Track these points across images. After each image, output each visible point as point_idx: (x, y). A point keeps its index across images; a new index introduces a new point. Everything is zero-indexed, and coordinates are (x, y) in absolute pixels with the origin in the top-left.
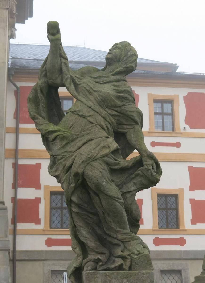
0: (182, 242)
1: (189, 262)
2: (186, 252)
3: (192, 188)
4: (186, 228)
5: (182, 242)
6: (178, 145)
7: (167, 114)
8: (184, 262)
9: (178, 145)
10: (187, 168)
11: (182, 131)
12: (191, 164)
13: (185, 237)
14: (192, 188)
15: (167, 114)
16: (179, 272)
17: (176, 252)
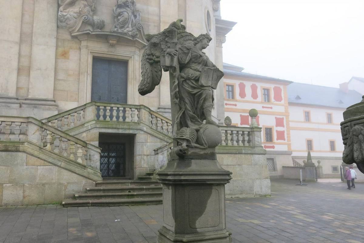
0: (273, 147)
1: (276, 155)
2: (276, 152)
3: (277, 126)
4: (275, 142)
5: (273, 147)
6: (271, 108)
7: (266, 95)
8: (274, 155)
9: (271, 108)
10: (275, 118)
11: (273, 102)
12: (276, 116)
13: (275, 145)
14: (277, 126)
15: (266, 95)
16: (272, 159)
17: (272, 151)
